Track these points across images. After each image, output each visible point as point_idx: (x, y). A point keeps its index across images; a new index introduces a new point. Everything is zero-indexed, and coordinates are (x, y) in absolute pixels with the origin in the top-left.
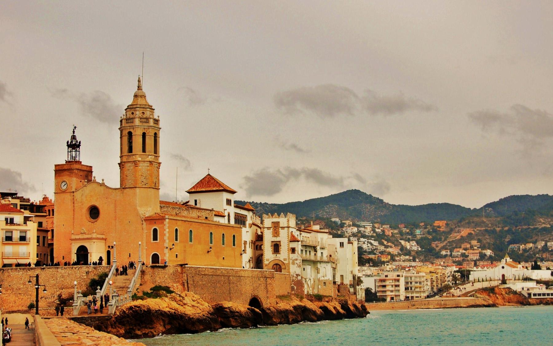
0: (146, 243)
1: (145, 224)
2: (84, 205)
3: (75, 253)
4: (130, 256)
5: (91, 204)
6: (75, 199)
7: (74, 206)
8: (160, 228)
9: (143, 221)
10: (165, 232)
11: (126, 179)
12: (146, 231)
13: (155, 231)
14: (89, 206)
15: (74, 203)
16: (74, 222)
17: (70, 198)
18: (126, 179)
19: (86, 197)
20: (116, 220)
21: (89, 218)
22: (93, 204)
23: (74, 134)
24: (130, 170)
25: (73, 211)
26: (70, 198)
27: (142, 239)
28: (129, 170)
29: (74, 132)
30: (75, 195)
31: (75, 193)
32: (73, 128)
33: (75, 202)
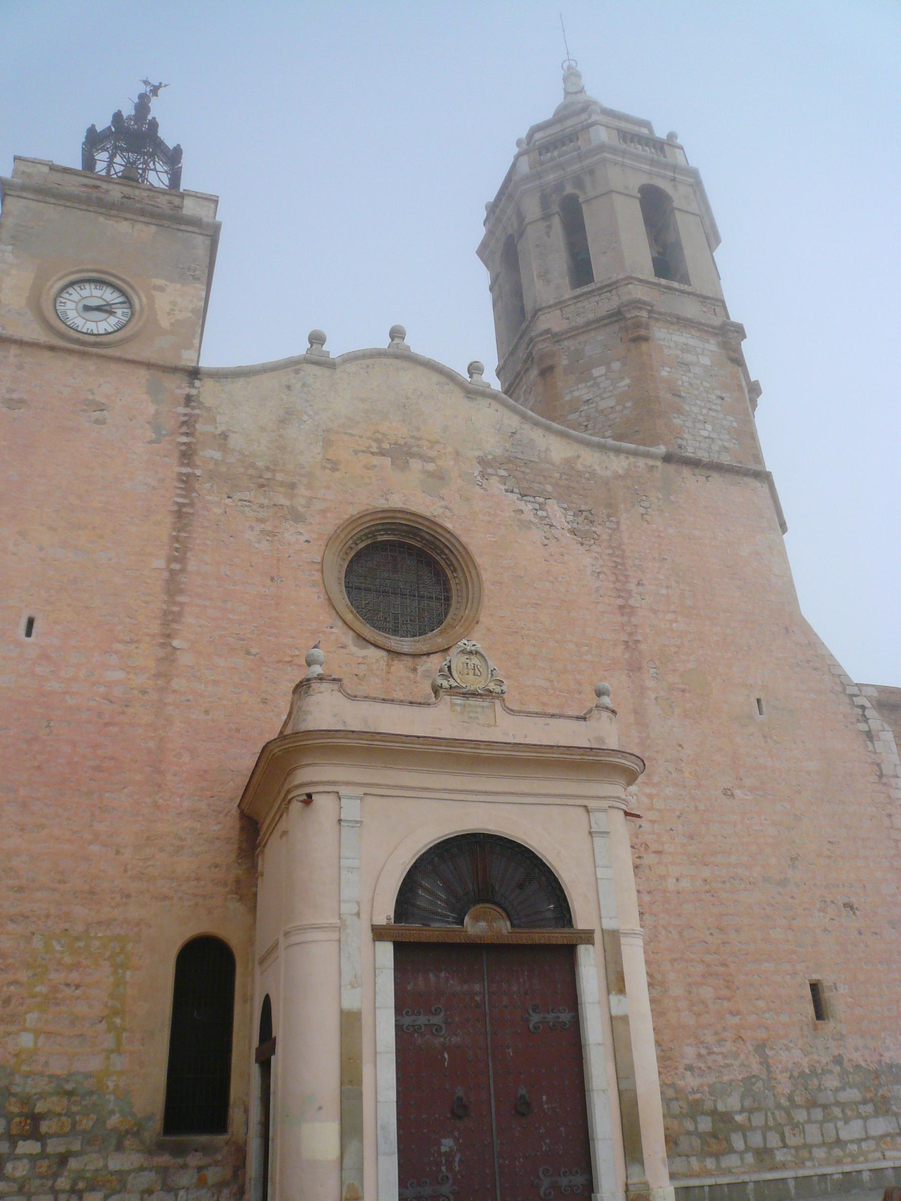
2: (302, 491)
3: (379, 933)
4: (820, 1012)
5: (382, 504)
11: (679, 411)
14: (353, 511)
15: (187, 455)
17: (152, 409)
18: (679, 411)
19: (327, 444)
20: (634, 668)
21: (349, 617)
22: (396, 502)
24: (696, 370)
25: (169, 520)
26: (152, 409)
33: (209, 453)
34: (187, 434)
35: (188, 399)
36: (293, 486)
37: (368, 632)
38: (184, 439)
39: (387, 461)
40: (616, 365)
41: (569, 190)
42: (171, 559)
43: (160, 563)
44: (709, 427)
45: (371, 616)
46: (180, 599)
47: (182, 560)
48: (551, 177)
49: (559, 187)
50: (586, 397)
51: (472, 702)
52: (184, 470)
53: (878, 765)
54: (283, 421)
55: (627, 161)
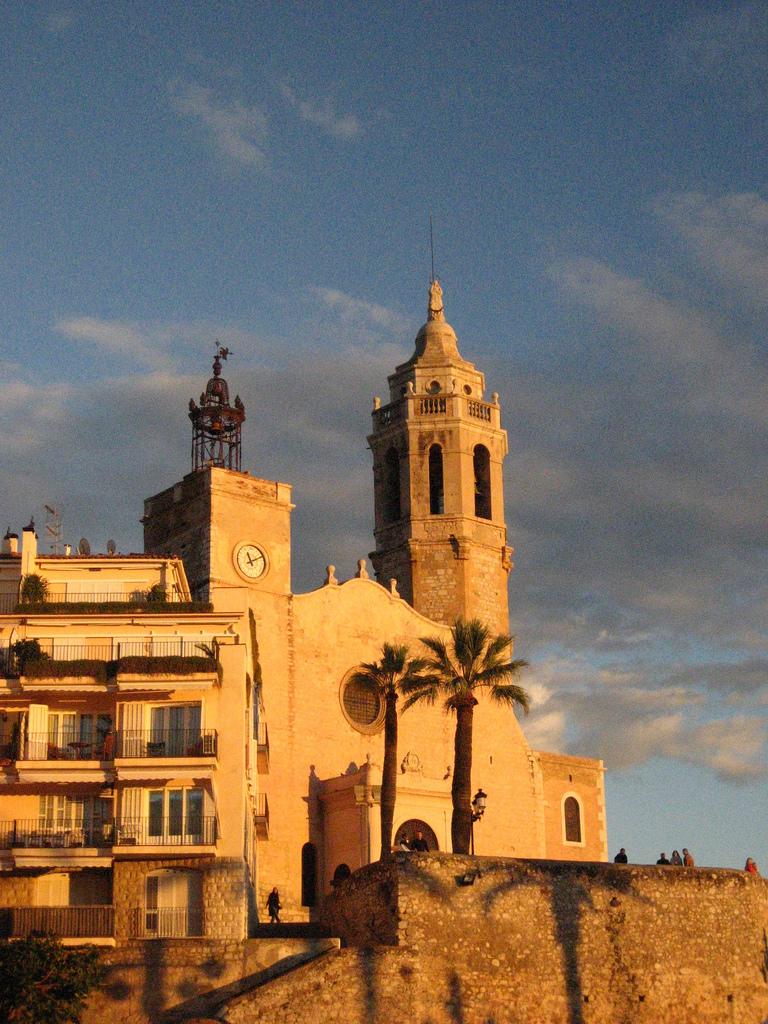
0: (547, 843)
1: (540, 776)
6: (295, 626)
7: (292, 654)
8: (586, 798)
9: (535, 764)
10: (600, 814)
11: (475, 603)
12: (545, 803)
13: (572, 806)
15: (291, 641)
16: (291, 719)
19: (338, 633)
23: (219, 377)
25: (288, 673)
27: (535, 828)
28: (483, 575)
29: (217, 368)
30: (295, 611)
31: (294, 602)
32: (216, 352)
33: (298, 640)
34: (290, 630)
35: (289, 611)
36: (327, 656)
37: (356, 725)
38: (290, 633)
39: (360, 640)
40: (450, 571)
41: (436, 440)
42: (289, 692)
43: (286, 694)
44: (488, 613)
45: (357, 720)
46: (294, 710)
47: (292, 692)
48: (427, 427)
49: (431, 435)
50: (433, 585)
51: (414, 773)
52: (291, 649)
53: (534, 789)
54: (323, 622)
55: (471, 429)
